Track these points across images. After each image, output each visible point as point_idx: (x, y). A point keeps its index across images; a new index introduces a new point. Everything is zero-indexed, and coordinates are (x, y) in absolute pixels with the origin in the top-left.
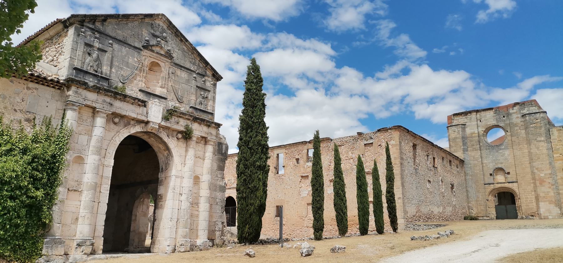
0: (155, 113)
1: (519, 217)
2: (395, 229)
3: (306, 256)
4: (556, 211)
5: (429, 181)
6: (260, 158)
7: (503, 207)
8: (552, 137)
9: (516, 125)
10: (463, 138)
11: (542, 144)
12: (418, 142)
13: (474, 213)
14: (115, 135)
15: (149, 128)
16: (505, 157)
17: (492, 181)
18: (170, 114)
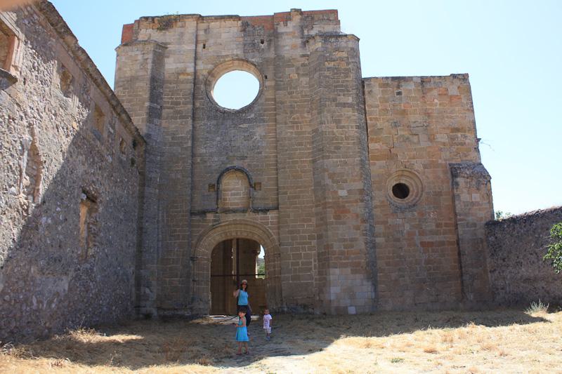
8: (369, 100)
9: (289, 63)
10: (153, 79)
11: (349, 112)
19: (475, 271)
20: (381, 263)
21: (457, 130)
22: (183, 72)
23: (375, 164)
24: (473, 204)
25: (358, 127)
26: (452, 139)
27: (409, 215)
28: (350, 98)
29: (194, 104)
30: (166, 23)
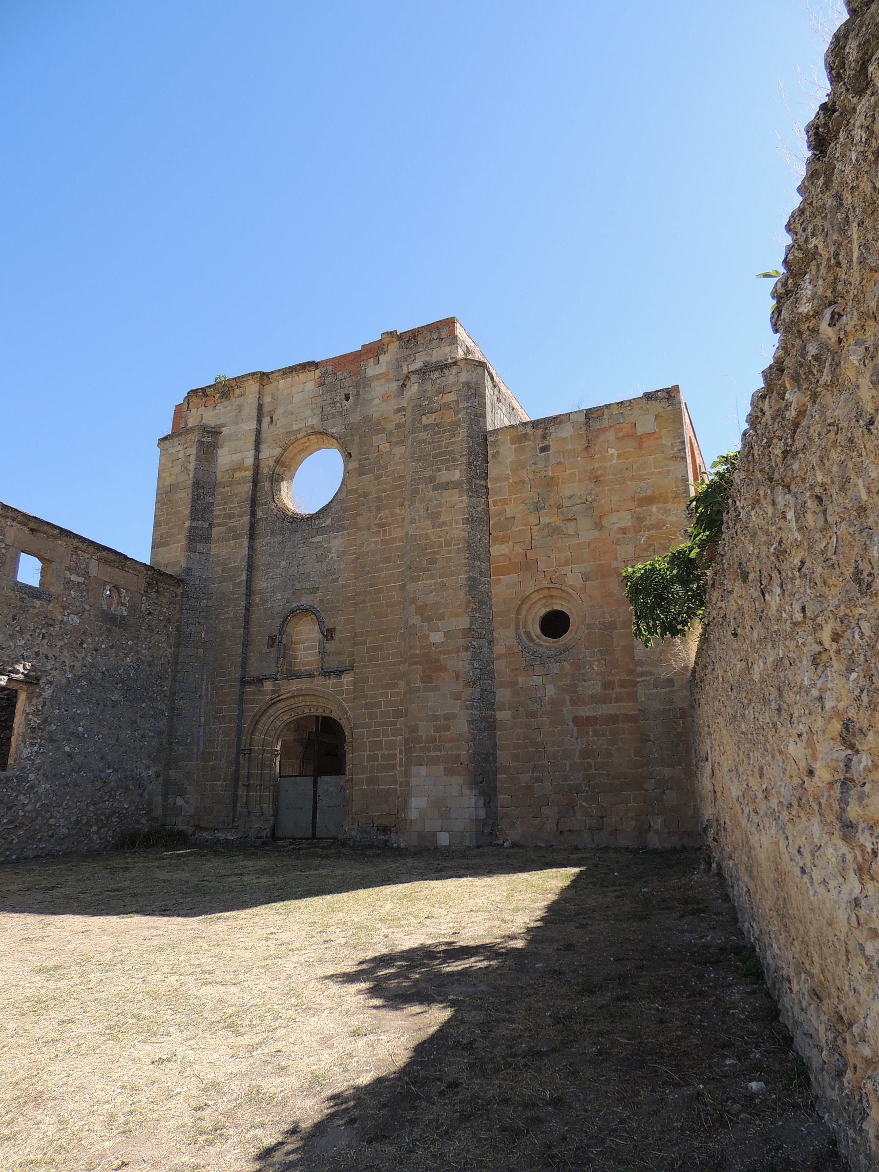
8: (494, 469)
10: (197, 485)
19: (667, 772)
21: (649, 500)
22: (240, 467)
23: (499, 582)
25: (466, 521)
26: (640, 519)
27: (555, 668)
28: (457, 472)
29: (253, 514)
30: (224, 390)
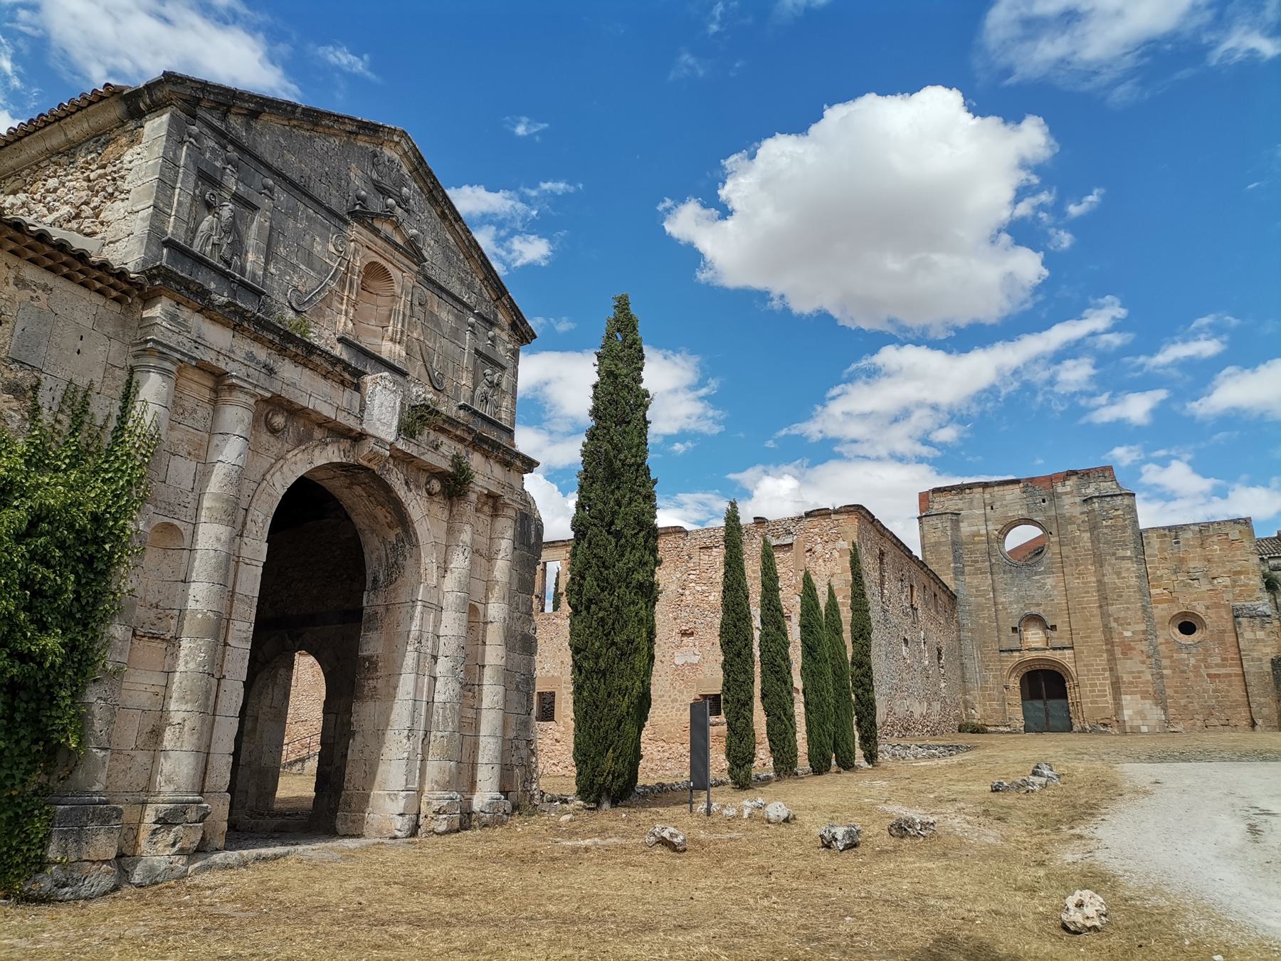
0: (382, 409)
1: (1075, 729)
2: (871, 757)
3: (848, 847)
4: (1156, 714)
5: (905, 640)
6: (643, 564)
7: (1039, 704)
9: (1071, 520)
10: (954, 543)
12: (887, 547)
13: (977, 716)
14: (272, 466)
15: (362, 455)
16: (1048, 589)
17: (1017, 645)
18: (418, 419)
19: (1262, 700)
20: (1169, 692)
21: (1240, 573)
24: (1258, 641)
